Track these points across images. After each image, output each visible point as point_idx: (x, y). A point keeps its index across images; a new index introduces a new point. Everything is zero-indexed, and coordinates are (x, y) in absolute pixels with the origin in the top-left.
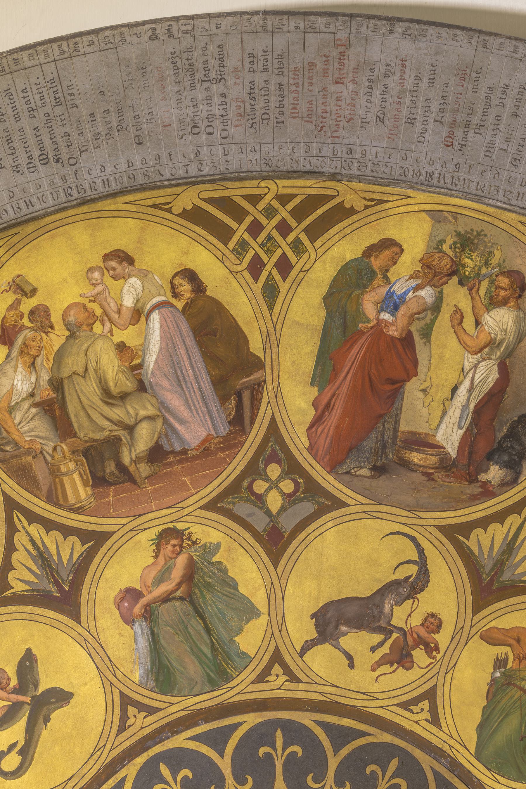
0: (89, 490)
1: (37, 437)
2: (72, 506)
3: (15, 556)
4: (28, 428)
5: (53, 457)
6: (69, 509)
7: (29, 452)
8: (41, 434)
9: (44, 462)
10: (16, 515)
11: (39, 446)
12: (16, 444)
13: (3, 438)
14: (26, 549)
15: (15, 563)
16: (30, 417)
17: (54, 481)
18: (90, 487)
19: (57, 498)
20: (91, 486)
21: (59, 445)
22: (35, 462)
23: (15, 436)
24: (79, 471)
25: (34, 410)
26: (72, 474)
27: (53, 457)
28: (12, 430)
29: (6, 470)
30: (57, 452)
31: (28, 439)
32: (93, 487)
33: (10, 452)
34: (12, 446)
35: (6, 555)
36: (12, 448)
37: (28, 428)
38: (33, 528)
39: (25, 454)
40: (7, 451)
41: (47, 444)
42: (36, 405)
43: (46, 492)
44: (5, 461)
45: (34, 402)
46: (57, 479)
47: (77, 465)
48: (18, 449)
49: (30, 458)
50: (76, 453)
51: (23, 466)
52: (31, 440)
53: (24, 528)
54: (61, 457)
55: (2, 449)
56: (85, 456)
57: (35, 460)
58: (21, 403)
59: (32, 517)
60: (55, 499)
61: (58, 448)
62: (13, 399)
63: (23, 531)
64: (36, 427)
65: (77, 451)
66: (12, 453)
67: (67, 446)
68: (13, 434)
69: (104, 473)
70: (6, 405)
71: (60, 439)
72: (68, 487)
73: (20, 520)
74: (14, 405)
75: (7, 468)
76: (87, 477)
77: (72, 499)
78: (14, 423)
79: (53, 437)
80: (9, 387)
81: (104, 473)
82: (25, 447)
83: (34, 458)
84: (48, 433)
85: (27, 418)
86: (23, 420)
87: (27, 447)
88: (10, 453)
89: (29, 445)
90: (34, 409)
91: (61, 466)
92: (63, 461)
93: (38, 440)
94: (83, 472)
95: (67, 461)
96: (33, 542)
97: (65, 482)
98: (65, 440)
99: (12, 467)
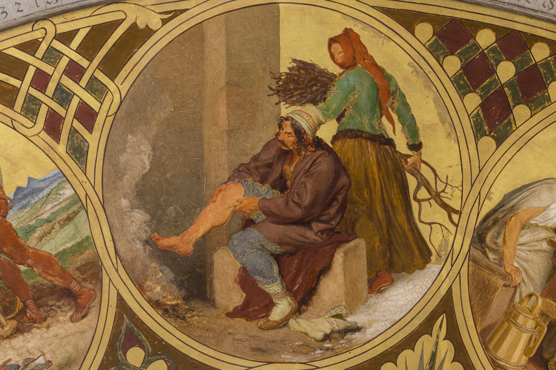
0: (524, 359)
1: (526, 271)
2: (497, 359)
3: (407, 353)
4: (525, 255)
5: (521, 301)
6: (492, 359)
7: (505, 276)
8: (530, 272)
9: (509, 298)
10: (442, 319)
11: (518, 280)
12: (502, 259)
13: (496, 243)
14: (422, 357)
15: (401, 359)
16: (536, 248)
17: (503, 323)
18: (527, 359)
19: (491, 339)
20: (529, 358)
21: (536, 296)
22: (502, 290)
23: (507, 252)
24: (532, 335)
25: (545, 246)
26: (523, 332)
27: (521, 301)
28: (510, 243)
29: (471, 273)
30: (529, 300)
31: (516, 264)
32: (531, 360)
33: (490, 260)
34: (496, 257)
35: (400, 344)
36: (495, 259)
37: (525, 255)
38: (446, 344)
39: (501, 275)
40: (488, 257)
41: (528, 285)
42: (551, 242)
43: (487, 325)
44: (478, 265)
45: (552, 239)
46: (506, 324)
47: (535, 328)
48: (498, 265)
49: (501, 282)
50: (545, 318)
51: (489, 283)
52: (518, 268)
53: (438, 337)
54: (528, 308)
55: (485, 251)
56: (550, 327)
57: (504, 288)
58: (540, 229)
59: (453, 335)
60: (487, 339)
61: (534, 298)
62: (537, 218)
63: (435, 339)
64: (532, 261)
65: (547, 316)
66: (490, 263)
67: (543, 304)
68: (507, 248)
69: (551, 358)
70: (526, 217)
71: (542, 292)
72: (509, 339)
73: (441, 327)
74: (532, 224)
75: (474, 272)
76: (533, 347)
77: (501, 353)
78: (517, 240)
79: (539, 283)
80: (544, 205)
81: (551, 358)
82: (507, 270)
83: (505, 285)
84: (538, 277)
85: (533, 246)
86: (528, 245)
87: (508, 270)
88: (488, 262)
89: (511, 271)
90: (546, 244)
91: (521, 316)
92: (526, 313)
93: (524, 274)
94: (534, 339)
95: (530, 317)
96: (434, 356)
97: (511, 332)
98: (546, 297)
99: (479, 275)
